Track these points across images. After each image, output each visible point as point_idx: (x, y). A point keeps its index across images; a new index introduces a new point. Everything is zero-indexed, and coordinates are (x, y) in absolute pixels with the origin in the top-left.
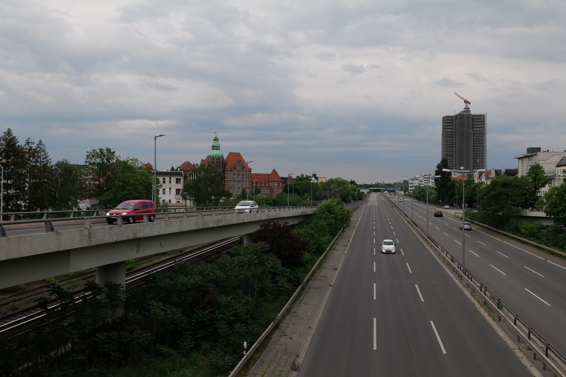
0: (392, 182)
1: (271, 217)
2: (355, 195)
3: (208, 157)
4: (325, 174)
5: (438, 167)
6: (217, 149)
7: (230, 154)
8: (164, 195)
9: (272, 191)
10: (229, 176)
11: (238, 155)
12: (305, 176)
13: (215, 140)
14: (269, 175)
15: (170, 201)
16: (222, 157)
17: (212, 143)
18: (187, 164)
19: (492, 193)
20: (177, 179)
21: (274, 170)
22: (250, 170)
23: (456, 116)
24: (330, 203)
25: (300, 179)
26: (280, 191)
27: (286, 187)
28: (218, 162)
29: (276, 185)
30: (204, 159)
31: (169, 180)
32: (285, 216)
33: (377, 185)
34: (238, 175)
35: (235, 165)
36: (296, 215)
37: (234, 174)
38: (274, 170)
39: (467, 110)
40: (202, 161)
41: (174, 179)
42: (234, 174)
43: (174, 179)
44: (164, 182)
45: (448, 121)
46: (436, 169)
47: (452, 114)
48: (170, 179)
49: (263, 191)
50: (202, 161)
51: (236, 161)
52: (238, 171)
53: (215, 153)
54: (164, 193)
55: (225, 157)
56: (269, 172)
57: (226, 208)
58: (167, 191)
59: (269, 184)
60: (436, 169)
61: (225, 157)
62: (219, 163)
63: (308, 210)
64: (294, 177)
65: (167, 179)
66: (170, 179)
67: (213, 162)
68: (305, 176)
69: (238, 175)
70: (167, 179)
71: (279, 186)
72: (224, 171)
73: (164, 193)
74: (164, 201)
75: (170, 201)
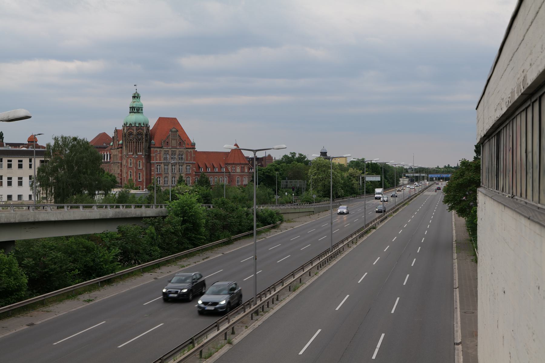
0: (431, 164)
2: (355, 186)
3: (125, 124)
4: (346, 151)
6: (138, 112)
7: (160, 119)
8: (20, 188)
9: (231, 179)
10: (158, 156)
11: (174, 121)
12: (297, 156)
13: (134, 97)
14: (226, 154)
16: (147, 126)
17: (129, 102)
19: (460, 181)
20: (42, 162)
22: (193, 146)
24: (185, 199)
25: (288, 160)
26: (246, 181)
28: (138, 134)
29: (238, 170)
30: (120, 128)
31: (28, 163)
32: (53, 219)
33: (421, 170)
34: (174, 153)
35: (168, 137)
36: (98, 217)
37: (166, 153)
40: (116, 131)
42: (166, 153)
43: (37, 162)
44: (20, 166)
48: (30, 161)
49: (213, 180)
50: (116, 131)
51: (170, 132)
52: (173, 147)
53: (134, 118)
54: (20, 184)
55: (152, 125)
57: (78, 207)
58: (15, 181)
59: (227, 169)
61: (152, 125)
62: (141, 134)
64: (277, 156)
65: (26, 161)
66: (30, 161)
67: (131, 134)
68: (297, 156)
69: (174, 153)
70: (26, 161)
71: (242, 171)
72: (149, 148)
73: (20, 184)
74: (20, 197)
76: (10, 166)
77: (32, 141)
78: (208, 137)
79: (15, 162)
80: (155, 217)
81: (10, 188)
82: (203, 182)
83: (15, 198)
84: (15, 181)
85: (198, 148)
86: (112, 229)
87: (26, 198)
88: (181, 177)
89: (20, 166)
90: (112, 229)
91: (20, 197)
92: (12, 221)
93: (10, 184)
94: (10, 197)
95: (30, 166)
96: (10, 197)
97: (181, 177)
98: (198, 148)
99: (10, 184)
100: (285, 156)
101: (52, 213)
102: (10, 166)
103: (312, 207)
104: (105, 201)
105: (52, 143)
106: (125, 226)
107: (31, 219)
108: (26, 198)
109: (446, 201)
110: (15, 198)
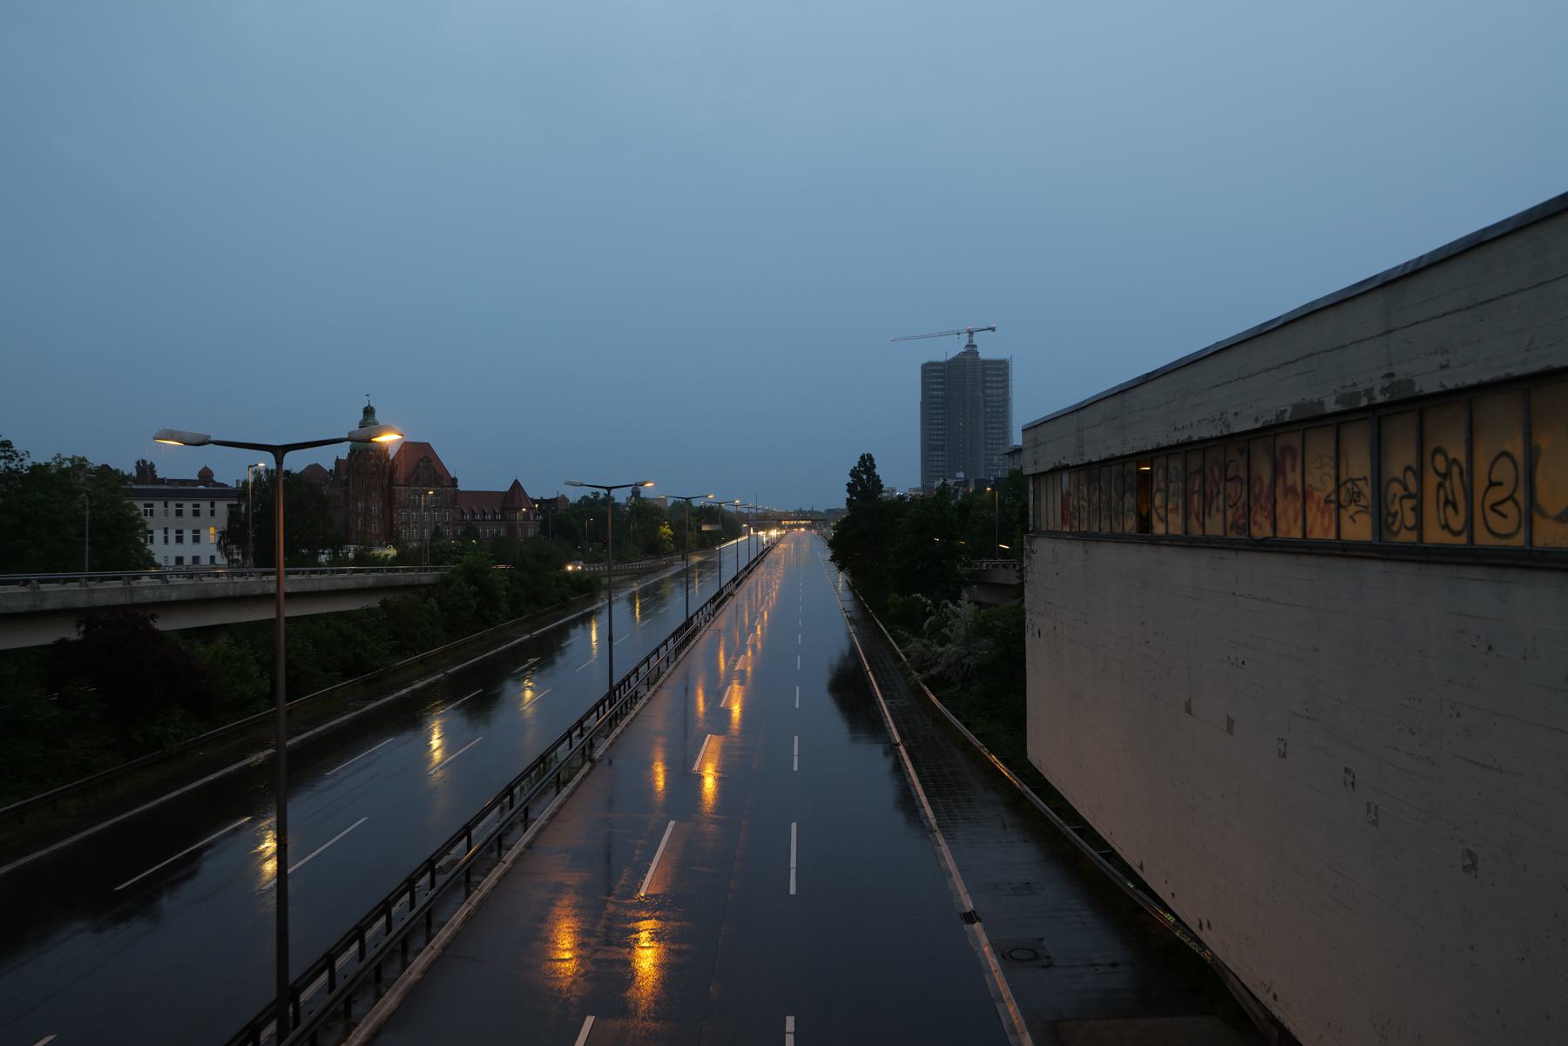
1: (218, 593)
5: (854, 473)
8: (197, 546)
9: (511, 529)
11: (426, 447)
15: (212, 558)
18: (317, 466)
21: (516, 484)
22: (454, 481)
23: (949, 362)
26: (531, 532)
27: (544, 521)
38: (516, 484)
39: (972, 348)
40: (338, 461)
41: (222, 507)
43: (222, 507)
44: (196, 514)
45: (929, 370)
46: (849, 480)
47: (941, 358)
51: (422, 461)
54: (196, 539)
56: (506, 489)
60: (849, 480)
63: (427, 577)
70: (205, 506)
73: (196, 539)
74: (196, 559)
75: (212, 558)
76: (179, 513)
77: (206, 475)
78: (476, 472)
79: (188, 507)
80: (434, 585)
81: (180, 547)
82: (470, 532)
83: (188, 561)
84: (188, 535)
85: (462, 486)
86: (374, 602)
87: (205, 561)
88: (437, 528)
89: (196, 514)
90: (374, 602)
91: (196, 559)
92: (231, 593)
93: (179, 540)
94: (179, 560)
95: (212, 513)
96: (179, 560)
97: (437, 528)
98: (462, 486)
99: (179, 540)
100: (585, 498)
101: (255, 582)
102: (179, 513)
103: (636, 565)
104: (330, 563)
105: (251, 479)
106: (389, 597)
107: (258, 591)
108: (205, 561)
109: (833, 559)
110: (188, 561)
